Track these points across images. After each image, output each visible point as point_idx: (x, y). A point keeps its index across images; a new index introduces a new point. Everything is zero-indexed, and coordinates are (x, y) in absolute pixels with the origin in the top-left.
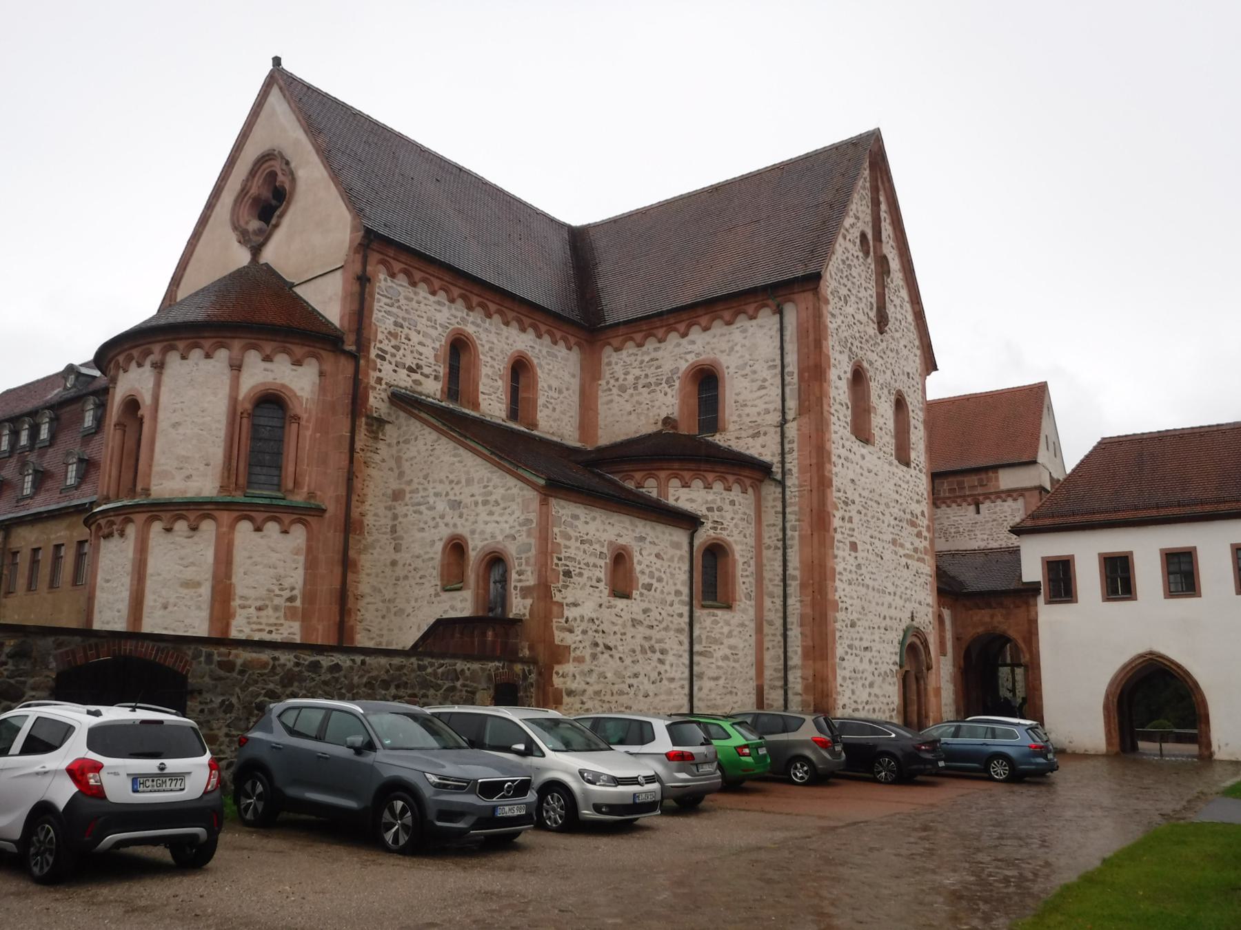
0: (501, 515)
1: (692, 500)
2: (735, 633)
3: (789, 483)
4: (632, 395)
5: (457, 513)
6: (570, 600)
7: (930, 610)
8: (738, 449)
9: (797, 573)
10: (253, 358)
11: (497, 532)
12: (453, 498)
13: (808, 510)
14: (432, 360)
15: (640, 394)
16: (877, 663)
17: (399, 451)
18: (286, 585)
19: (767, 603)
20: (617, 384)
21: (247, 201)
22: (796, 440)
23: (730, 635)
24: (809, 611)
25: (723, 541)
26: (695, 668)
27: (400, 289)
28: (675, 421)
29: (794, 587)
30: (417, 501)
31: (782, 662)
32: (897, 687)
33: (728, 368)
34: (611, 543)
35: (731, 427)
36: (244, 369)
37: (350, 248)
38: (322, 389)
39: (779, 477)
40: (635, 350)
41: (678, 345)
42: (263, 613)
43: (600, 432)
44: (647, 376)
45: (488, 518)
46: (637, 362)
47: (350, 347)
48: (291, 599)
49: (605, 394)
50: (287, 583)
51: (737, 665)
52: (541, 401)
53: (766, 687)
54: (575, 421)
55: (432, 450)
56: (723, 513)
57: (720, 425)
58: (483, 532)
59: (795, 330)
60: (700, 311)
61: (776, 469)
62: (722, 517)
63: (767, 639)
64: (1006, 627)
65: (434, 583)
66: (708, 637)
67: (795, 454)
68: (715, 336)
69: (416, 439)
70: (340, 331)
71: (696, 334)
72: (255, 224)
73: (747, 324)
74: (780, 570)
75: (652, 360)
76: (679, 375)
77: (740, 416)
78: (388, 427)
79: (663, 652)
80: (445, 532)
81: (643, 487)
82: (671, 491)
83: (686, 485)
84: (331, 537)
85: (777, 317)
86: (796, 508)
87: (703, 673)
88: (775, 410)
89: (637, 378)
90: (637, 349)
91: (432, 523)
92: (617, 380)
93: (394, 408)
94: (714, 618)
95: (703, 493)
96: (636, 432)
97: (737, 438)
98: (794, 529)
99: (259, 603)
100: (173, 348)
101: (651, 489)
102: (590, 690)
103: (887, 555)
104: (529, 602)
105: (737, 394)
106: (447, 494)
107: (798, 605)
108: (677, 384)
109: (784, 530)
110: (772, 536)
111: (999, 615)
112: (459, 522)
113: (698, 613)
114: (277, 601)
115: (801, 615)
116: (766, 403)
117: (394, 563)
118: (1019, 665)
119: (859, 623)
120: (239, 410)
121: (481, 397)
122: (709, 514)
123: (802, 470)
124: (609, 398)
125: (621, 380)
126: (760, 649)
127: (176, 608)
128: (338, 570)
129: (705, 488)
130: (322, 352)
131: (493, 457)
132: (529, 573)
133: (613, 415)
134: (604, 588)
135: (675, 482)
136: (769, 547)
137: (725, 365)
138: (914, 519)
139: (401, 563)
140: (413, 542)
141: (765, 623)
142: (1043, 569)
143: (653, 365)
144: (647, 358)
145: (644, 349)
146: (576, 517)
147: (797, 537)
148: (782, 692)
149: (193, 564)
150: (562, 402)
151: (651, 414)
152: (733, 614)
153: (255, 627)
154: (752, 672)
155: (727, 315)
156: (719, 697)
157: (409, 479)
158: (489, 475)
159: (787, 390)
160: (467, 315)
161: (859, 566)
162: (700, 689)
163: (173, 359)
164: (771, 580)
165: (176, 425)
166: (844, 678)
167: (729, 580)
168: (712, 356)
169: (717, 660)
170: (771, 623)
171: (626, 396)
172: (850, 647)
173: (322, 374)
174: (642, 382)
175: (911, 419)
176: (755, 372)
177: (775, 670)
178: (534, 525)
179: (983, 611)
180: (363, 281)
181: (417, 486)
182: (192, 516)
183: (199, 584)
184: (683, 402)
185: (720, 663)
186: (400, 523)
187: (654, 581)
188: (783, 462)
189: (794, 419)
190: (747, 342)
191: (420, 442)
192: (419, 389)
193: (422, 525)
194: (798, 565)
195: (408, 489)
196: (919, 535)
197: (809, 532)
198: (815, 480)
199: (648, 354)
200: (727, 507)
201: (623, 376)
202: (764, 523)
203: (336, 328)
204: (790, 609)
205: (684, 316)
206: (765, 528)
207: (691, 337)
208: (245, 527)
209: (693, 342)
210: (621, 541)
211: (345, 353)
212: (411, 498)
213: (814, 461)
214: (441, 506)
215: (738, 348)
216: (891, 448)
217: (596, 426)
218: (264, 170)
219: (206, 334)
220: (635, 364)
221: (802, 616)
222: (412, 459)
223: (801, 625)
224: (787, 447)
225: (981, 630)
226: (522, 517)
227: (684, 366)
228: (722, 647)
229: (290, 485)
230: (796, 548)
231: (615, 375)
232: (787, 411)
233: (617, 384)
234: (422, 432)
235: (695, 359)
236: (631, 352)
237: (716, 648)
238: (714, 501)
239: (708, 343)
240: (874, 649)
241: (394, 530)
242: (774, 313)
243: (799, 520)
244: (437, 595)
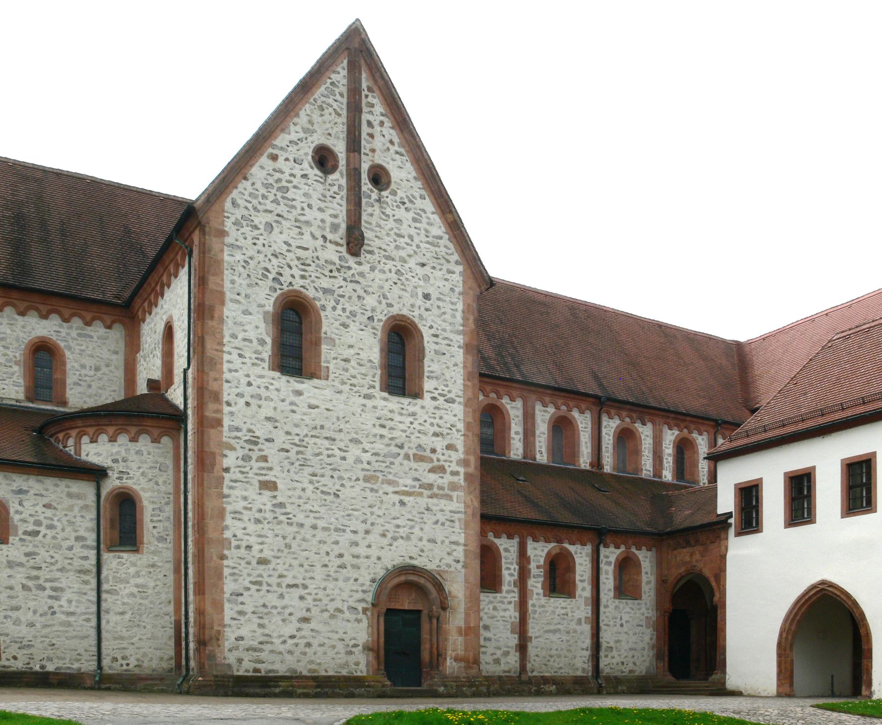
23: (137, 574)
25: (128, 489)
152: (139, 556)
156: (124, 630)
162: (108, 622)
169: (123, 597)
228: (128, 585)
237: (122, 586)
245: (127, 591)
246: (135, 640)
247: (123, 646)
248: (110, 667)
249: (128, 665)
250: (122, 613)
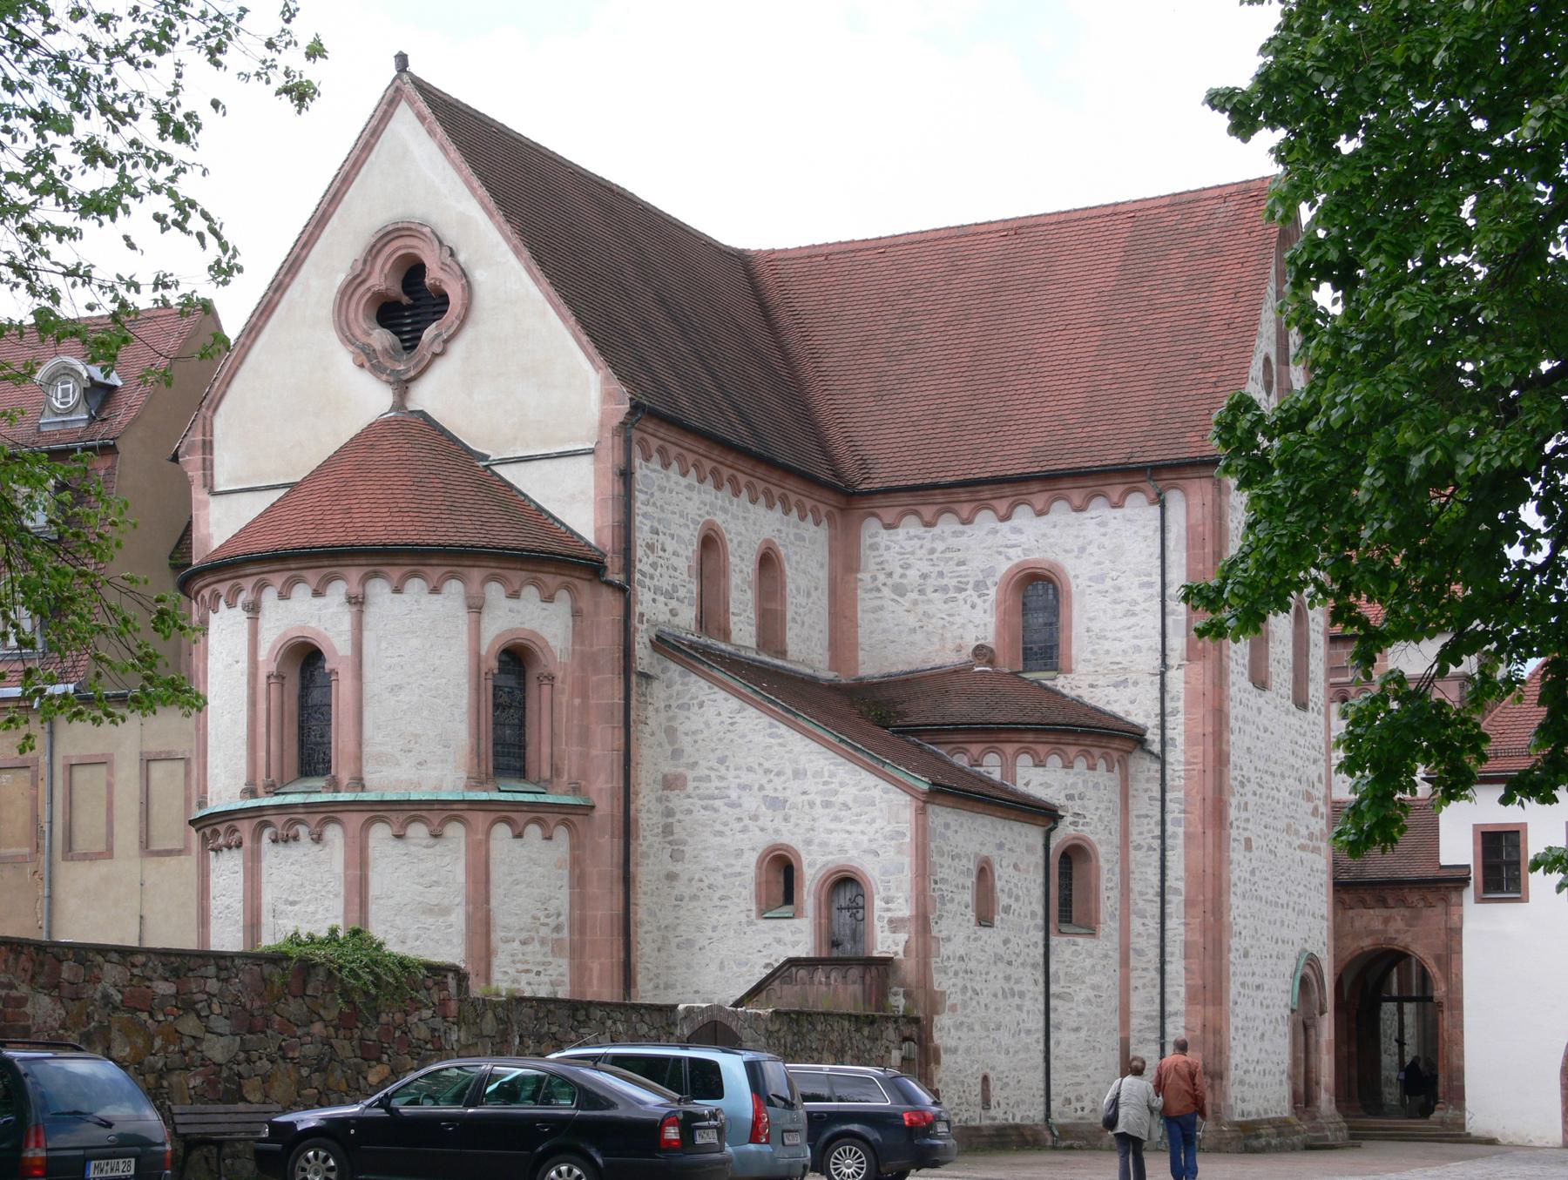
0: (853, 823)
1: (1047, 785)
2: (1099, 968)
3: (1170, 757)
4: (915, 603)
5: (779, 815)
6: (944, 934)
7: (1325, 924)
8: (1093, 703)
9: (1181, 885)
10: (495, 591)
11: (849, 845)
12: (772, 794)
13: (1199, 797)
14: (686, 577)
15: (929, 601)
16: (1268, 1007)
17: (670, 719)
18: (552, 910)
19: (1136, 924)
20: (890, 581)
21: (362, 296)
22: (1182, 696)
23: (1093, 970)
24: (1197, 937)
26: (1052, 1016)
27: (654, 475)
28: (992, 651)
29: (1175, 903)
30: (707, 792)
31: (1157, 1006)
32: (1287, 1040)
33: (1076, 577)
34: (976, 855)
35: (1079, 667)
36: (485, 610)
37: (602, 425)
38: (578, 634)
39: (1156, 748)
40: (921, 530)
41: (994, 532)
42: (530, 948)
43: (861, 655)
44: (941, 574)
45: (833, 826)
46: (924, 551)
47: (618, 578)
48: (558, 929)
49: (871, 596)
50: (553, 906)
51: (1099, 1011)
52: (789, 616)
53: (1132, 1041)
54: (824, 639)
55: (732, 724)
56: (1086, 802)
57: (1062, 664)
58: (824, 844)
59: (1183, 532)
60: (1035, 487)
61: (1153, 736)
62: (1084, 808)
63: (1133, 974)
64: (1409, 939)
65: (743, 906)
66: (1066, 973)
67: (1181, 718)
68: (1055, 526)
69: (701, 705)
70: (596, 549)
71: (1023, 516)
72: (381, 338)
73: (1109, 513)
74: (1156, 880)
75: (948, 549)
76: (997, 579)
77: (1093, 652)
78: (656, 684)
79: (1022, 995)
81: (981, 766)
82: (1020, 771)
83: (1040, 763)
84: (606, 846)
85: (1156, 509)
86: (1181, 795)
87: (1060, 1024)
88: (1150, 648)
89: (924, 576)
90: (924, 529)
91: (739, 826)
92: (890, 575)
93: (657, 656)
94: (1074, 948)
95: (1061, 773)
96: (923, 661)
97: (1092, 686)
98: (1177, 822)
99: (524, 935)
100: (376, 575)
101: (991, 768)
102: (962, 1046)
103: (1282, 849)
104: (902, 937)
105: (1091, 619)
106: (761, 788)
107: (1182, 929)
108: (992, 592)
109: (1163, 822)
110: (1144, 832)
111: (1399, 918)
112: (784, 827)
113: (1055, 940)
114: (544, 931)
115: (1186, 943)
116: (1136, 637)
117: (672, 877)
118: (1411, 999)
119: (1252, 952)
120: (484, 669)
121: (733, 619)
122: (1069, 803)
123: (1190, 741)
124: (878, 602)
125: (896, 576)
126: (1125, 989)
127: (418, 943)
128: (619, 889)
129: (1065, 767)
130: (577, 582)
131: (843, 746)
132: (901, 901)
133: (884, 631)
134: (971, 915)
135: (1025, 760)
136: (1138, 847)
137: (1071, 573)
138: (1310, 790)
139: (684, 877)
140: (705, 849)
141: (1131, 952)
142: (1475, 843)
143: (952, 558)
144: (940, 546)
145: (936, 530)
146: (947, 826)
147: (1182, 836)
148: (1158, 1047)
149: (437, 883)
150: (811, 611)
151: (949, 635)
152: (1095, 942)
153: (520, 966)
154: (1116, 1022)
155: (1077, 497)
156: (1079, 1054)
157: (692, 760)
158: (832, 767)
159: (1170, 620)
160: (716, 498)
161: (1253, 872)
162: (1058, 1043)
163: (379, 590)
164: (1141, 894)
165: (395, 689)
166: (1237, 1029)
167: (1091, 892)
168: (1050, 556)
169: (1078, 1005)
170: (1140, 953)
171: (905, 603)
172: (1243, 985)
173: (576, 613)
174: (932, 582)
175: (1311, 633)
176: (1119, 589)
177: (1147, 1017)
178: (907, 840)
179: (1371, 911)
180: (626, 475)
181: (707, 772)
182: (436, 818)
183: (445, 911)
184: (1003, 625)
185: (1081, 1010)
186: (679, 821)
187: (1012, 901)
188: (1163, 727)
189: (1180, 666)
190: (1106, 541)
191: (709, 712)
192: (676, 621)
193: (718, 827)
194: (1182, 873)
195: (690, 775)
196: (1315, 812)
197: (1201, 830)
198: (1210, 757)
199: (943, 539)
200: (1090, 793)
201: (900, 571)
202: (1133, 814)
203: (588, 544)
204: (1169, 934)
205: (1007, 490)
206: (1133, 819)
207: (1014, 522)
208: (502, 832)
209: (1020, 531)
210: (985, 852)
211: (610, 584)
212: (696, 788)
213: (1209, 729)
214: (751, 803)
215: (1092, 549)
216: (1287, 689)
217: (854, 646)
218: (395, 251)
219: (435, 561)
220: (920, 553)
221: (1187, 945)
222: (694, 733)
223: (1186, 957)
224: (1169, 706)
225: (1367, 943)
226: (889, 828)
227: (1003, 567)
228: (1083, 986)
229: (546, 773)
230: (1180, 850)
231: (885, 565)
232: (1168, 652)
233: (890, 581)
234: (712, 697)
235: (1023, 558)
236: (912, 532)
237: (1077, 989)
238: (1074, 785)
239: (1044, 535)
240: (1266, 987)
241: (668, 830)
242: (1152, 503)
243: (1185, 812)
244: (750, 923)
245: (1082, 996)
246: (1091, 1069)
247: (1078, 1080)
248: (1061, 1114)
249: (1083, 1109)
250: (1077, 1029)
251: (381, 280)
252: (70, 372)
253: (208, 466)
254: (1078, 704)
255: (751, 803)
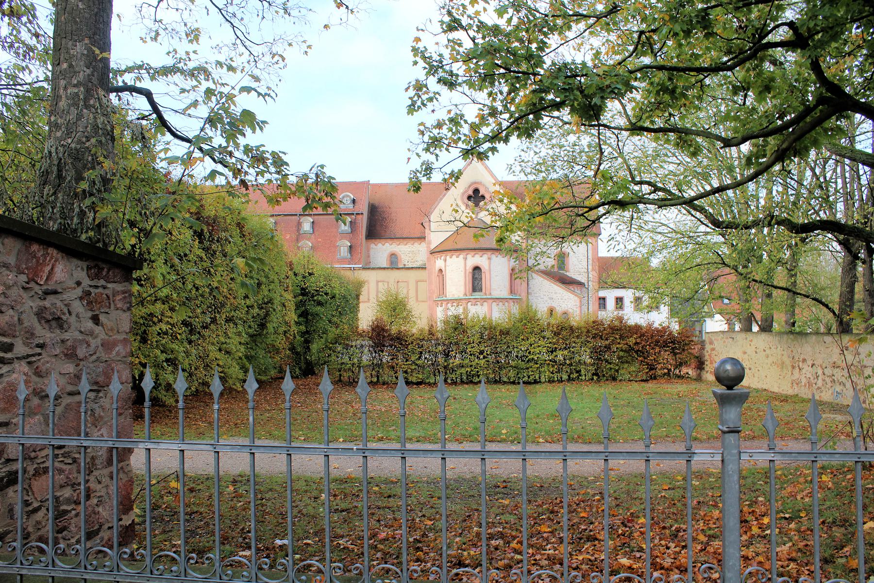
61: (586, 284)
80: (550, 305)
163: (493, 257)
191: (537, 280)
214: (546, 298)
251: (471, 193)
252: (348, 196)
253: (430, 226)
254: (571, 278)
255: (546, 298)
